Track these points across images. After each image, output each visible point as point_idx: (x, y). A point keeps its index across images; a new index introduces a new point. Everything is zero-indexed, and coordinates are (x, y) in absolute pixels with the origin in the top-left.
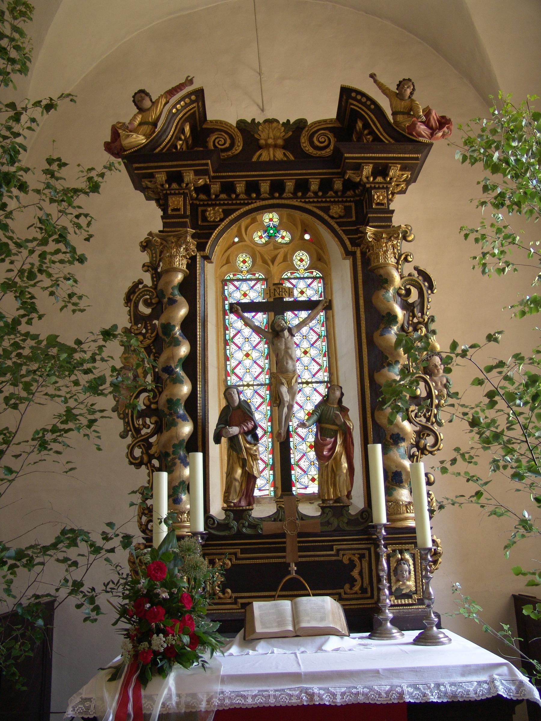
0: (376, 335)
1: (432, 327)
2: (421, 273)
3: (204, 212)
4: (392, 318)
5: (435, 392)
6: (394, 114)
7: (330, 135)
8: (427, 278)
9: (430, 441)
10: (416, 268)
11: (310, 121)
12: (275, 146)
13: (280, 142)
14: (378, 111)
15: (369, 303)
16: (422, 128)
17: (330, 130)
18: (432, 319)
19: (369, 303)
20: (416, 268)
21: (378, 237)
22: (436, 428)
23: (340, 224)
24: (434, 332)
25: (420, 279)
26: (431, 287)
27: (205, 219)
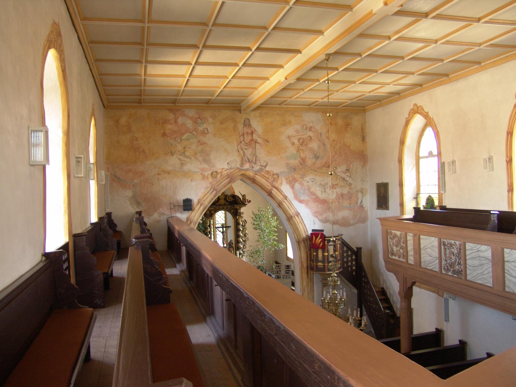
0: (238, 232)
1: (246, 229)
2: (245, 220)
3: (211, 211)
4: (240, 230)
5: (246, 239)
6: (243, 199)
7: (232, 197)
8: (246, 221)
9: (245, 247)
10: (244, 220)
11: (228, 194)
12: (223, 200)
13: (223, 199)
14: (240, 198)
15: (237, 227)
16: (247, 202)
17: (232, 196)
18: (246, 228)
19: (237, 227)
20: (244, 220)
21: (239, 217)
22: (246, 245)
23: (232, 213)
24: (246, 230)
25: (245, 221)
26: (246, 223)
27: (211, 212)
